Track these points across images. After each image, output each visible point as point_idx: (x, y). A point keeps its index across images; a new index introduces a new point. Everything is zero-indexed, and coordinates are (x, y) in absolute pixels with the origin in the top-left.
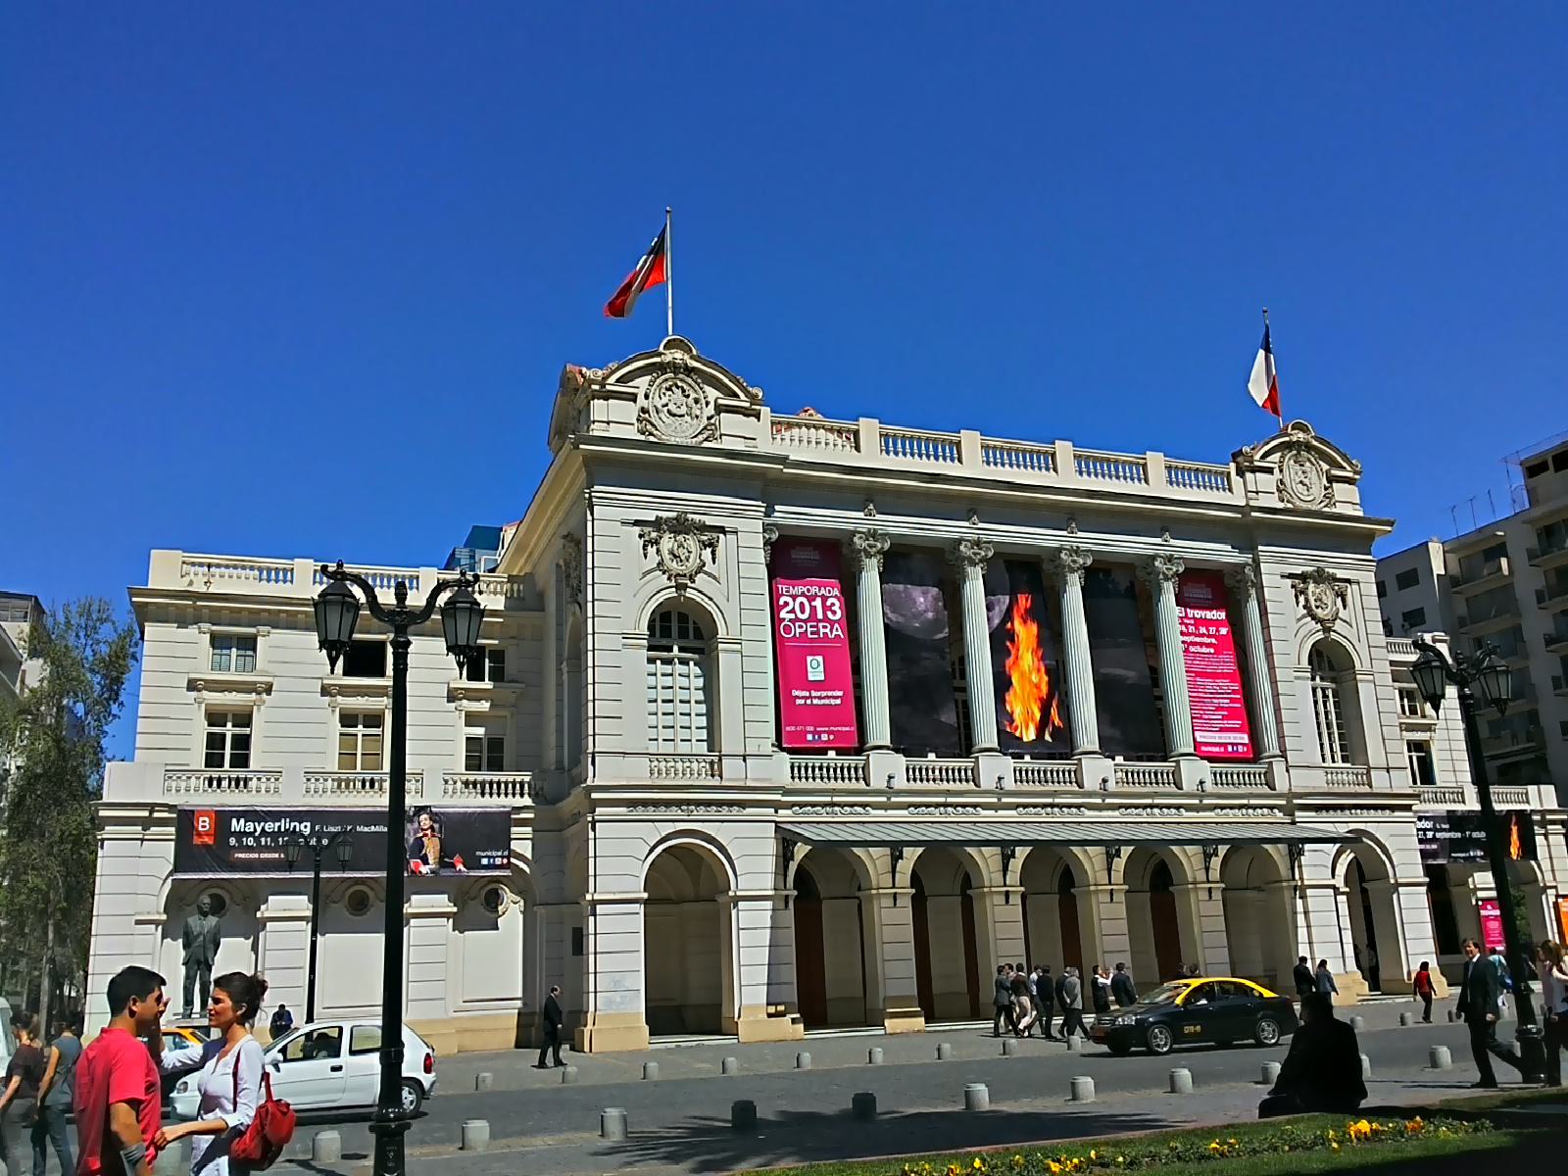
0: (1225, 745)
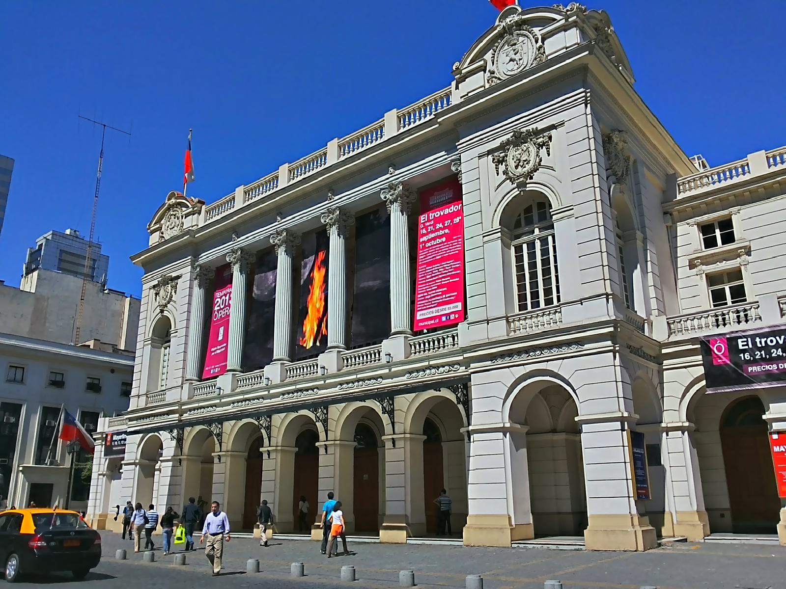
0: (440, 317)
